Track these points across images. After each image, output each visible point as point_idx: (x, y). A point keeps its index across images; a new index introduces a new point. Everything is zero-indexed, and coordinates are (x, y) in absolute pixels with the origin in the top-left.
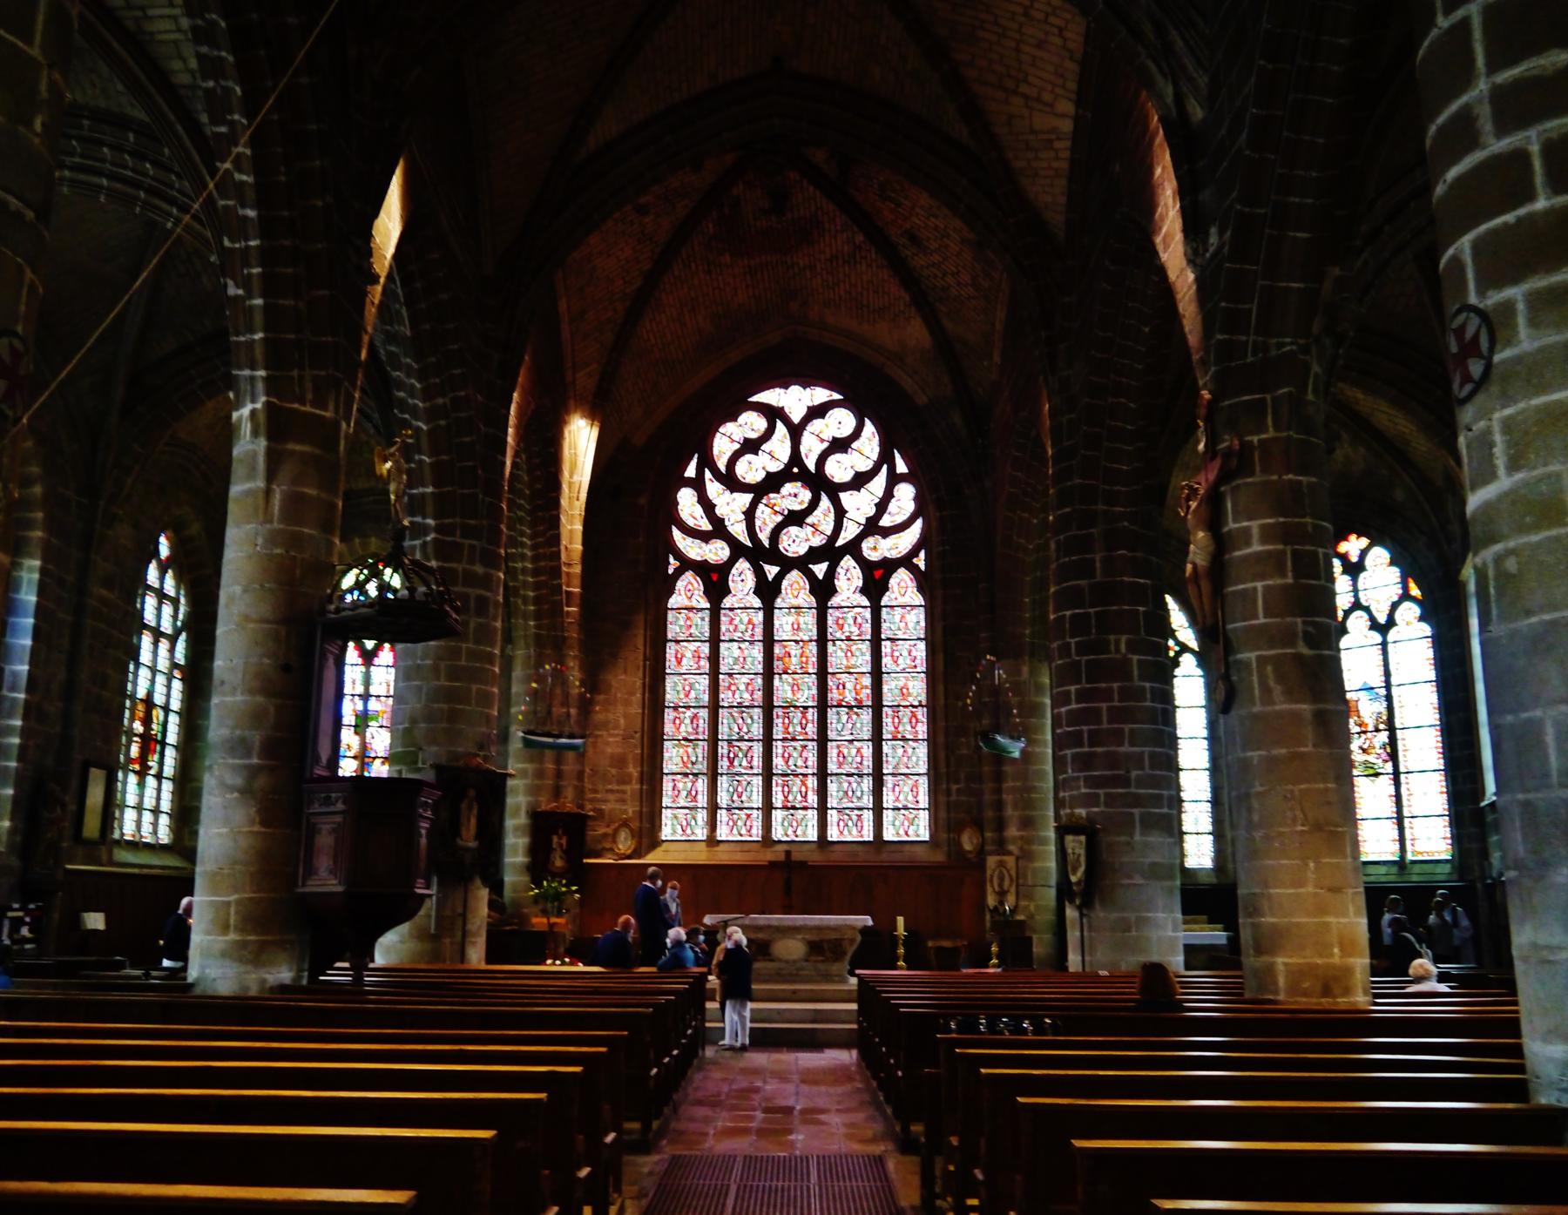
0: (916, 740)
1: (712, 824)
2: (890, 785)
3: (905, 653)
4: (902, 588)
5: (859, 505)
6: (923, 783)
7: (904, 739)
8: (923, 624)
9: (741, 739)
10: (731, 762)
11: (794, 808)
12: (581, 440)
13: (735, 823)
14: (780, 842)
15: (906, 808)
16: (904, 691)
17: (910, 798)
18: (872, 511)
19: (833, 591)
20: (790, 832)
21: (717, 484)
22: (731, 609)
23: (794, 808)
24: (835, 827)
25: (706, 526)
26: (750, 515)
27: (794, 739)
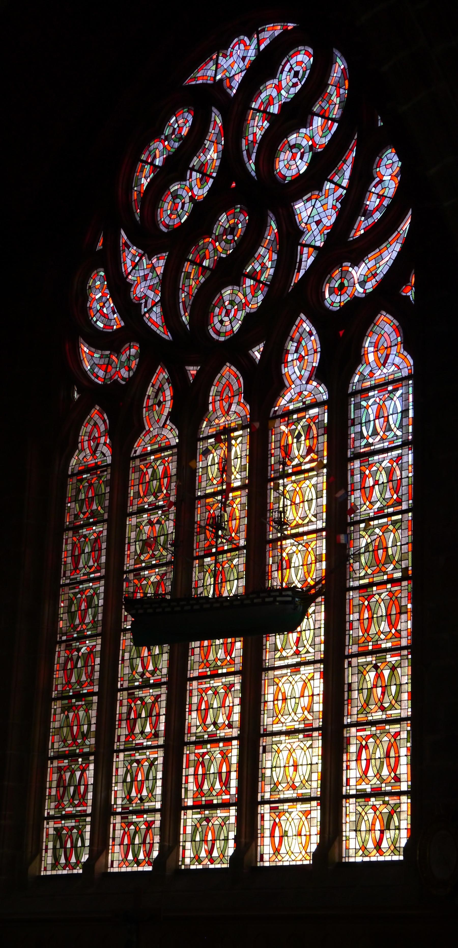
0: (395, 650)
1: (101, 844)
2: (353, 749)
3: (383, 478)
4: (385, 354)
5: (317, 215)
6: (404, 731)
7: (378, 651)
8: (411, 414)
9: (145, 685)
10: (132, 729)
11: (210, 806)
12: (99, 246)
13: (132, 842)
14: (188, 871)
15: (377, 793)
16: (378, 553)
17: (385, 772)
18: (330, 220)
19: (279, 386)
20: (203, 854)
21: (133, 249)
22: (144, 456)
23: (210, 806)
24: (267, 841)
25: (116, 322)
26: (169, 284)
27: (215, 676)
